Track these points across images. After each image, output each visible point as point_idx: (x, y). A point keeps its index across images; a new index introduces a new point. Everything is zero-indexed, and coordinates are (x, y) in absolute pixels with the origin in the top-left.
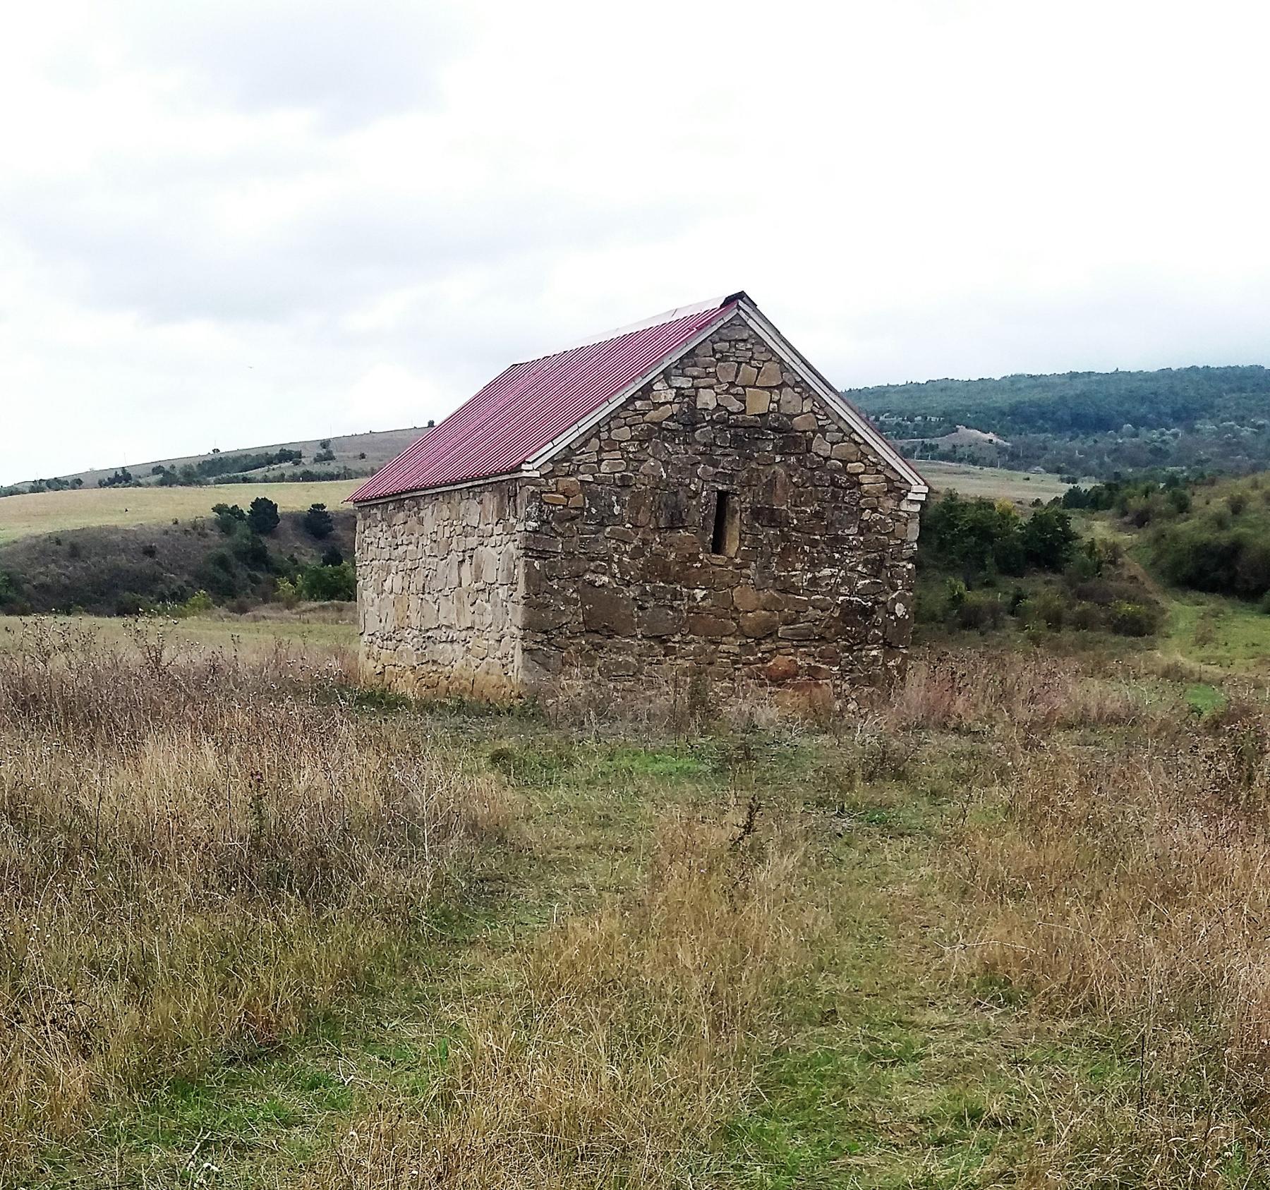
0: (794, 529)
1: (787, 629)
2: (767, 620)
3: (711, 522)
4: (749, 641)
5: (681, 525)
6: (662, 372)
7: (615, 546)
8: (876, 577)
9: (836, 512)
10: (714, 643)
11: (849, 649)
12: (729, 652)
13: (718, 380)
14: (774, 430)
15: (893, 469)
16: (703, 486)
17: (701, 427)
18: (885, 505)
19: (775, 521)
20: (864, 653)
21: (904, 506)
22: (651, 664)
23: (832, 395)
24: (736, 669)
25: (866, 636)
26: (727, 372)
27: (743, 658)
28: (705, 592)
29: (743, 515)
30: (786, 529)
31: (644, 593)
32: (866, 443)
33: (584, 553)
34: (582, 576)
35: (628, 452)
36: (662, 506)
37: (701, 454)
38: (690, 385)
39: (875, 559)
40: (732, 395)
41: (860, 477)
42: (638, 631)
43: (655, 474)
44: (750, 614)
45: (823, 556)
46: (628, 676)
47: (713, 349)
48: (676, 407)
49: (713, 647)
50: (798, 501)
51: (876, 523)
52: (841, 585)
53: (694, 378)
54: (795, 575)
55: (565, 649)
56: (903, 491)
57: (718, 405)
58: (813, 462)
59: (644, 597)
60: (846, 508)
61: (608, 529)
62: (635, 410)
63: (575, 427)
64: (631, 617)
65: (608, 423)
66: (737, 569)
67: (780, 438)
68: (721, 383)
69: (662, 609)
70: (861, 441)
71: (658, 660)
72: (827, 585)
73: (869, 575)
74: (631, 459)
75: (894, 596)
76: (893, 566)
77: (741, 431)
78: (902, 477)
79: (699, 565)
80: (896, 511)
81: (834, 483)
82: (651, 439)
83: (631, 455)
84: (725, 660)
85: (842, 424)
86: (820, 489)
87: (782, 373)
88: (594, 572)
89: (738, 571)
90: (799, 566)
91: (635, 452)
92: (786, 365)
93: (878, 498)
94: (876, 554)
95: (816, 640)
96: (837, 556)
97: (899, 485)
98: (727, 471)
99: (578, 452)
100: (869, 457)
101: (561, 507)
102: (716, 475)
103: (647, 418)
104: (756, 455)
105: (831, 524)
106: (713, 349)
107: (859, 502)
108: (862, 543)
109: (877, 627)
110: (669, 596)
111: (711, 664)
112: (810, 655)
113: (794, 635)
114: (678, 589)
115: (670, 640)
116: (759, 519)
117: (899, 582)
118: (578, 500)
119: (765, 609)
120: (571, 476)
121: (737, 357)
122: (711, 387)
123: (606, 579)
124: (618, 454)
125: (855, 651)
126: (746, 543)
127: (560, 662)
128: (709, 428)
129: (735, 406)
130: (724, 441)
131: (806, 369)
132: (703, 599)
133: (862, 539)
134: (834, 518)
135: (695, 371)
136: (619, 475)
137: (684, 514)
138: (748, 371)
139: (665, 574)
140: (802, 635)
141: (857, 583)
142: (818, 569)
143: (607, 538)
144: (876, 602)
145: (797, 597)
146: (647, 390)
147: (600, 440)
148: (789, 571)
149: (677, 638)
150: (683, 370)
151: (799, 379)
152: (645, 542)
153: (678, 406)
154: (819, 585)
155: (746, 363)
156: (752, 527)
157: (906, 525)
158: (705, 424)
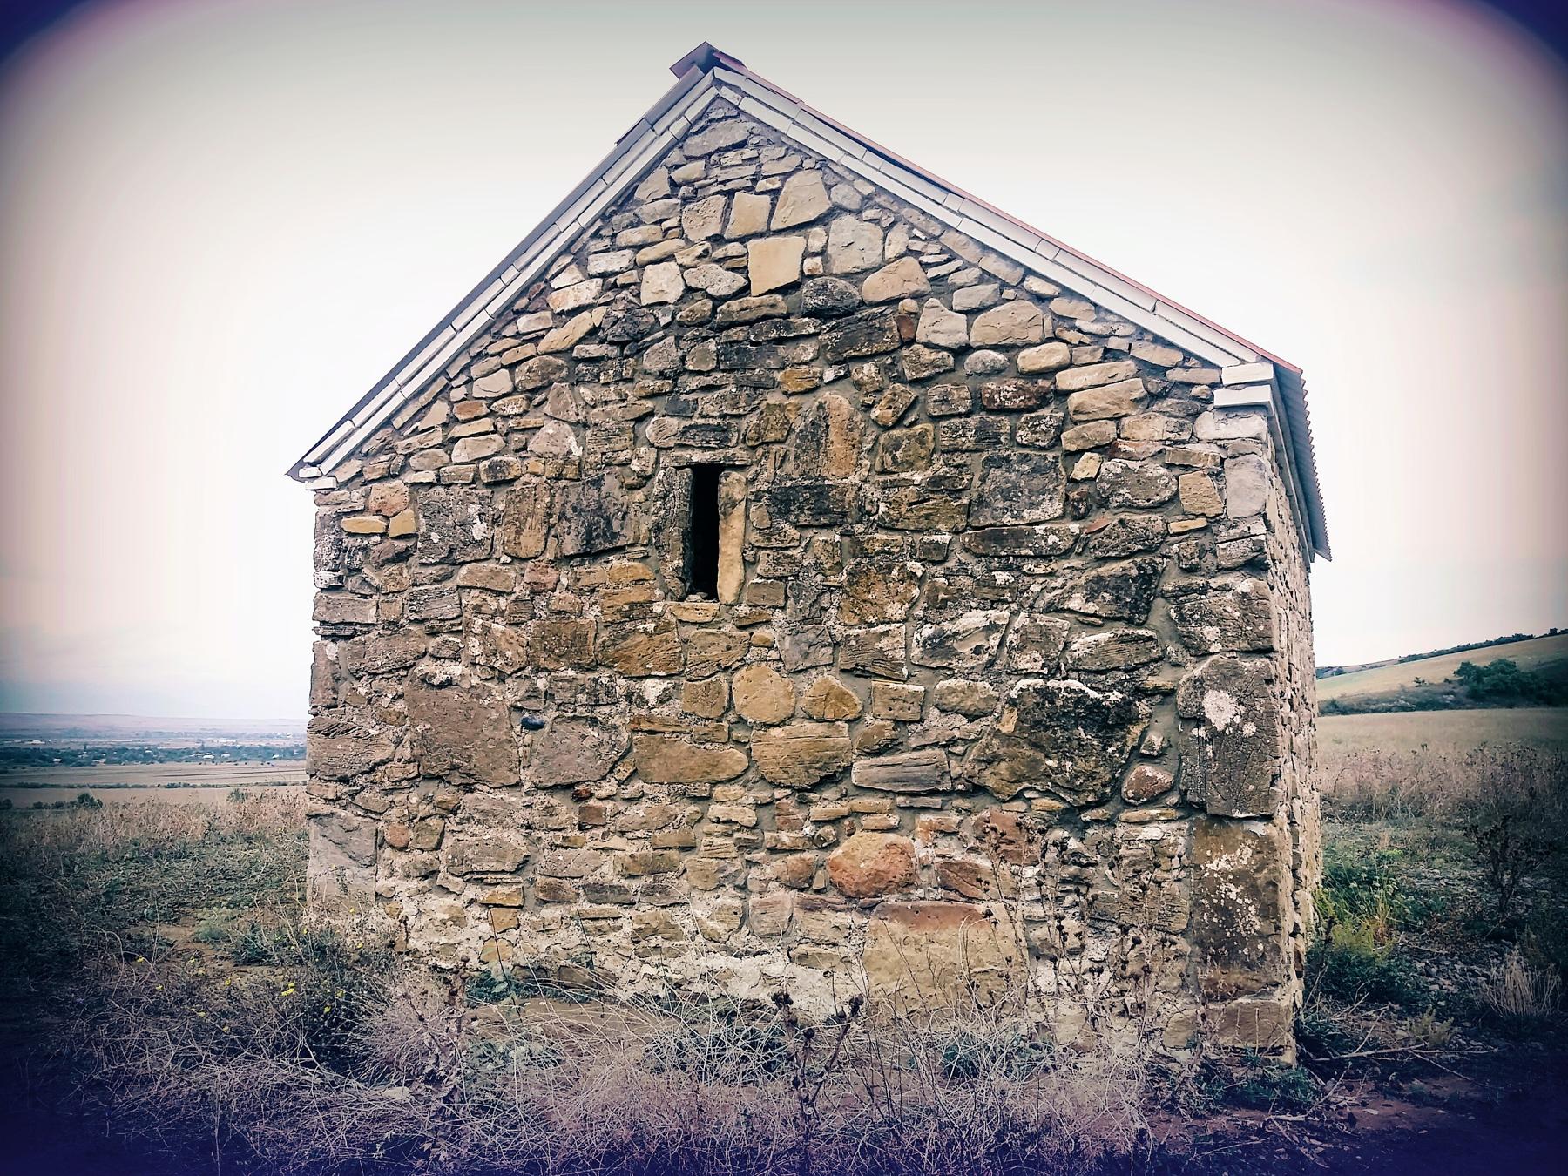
0: (881, 526)
1: (872, 766)
2: (816, 744)
3: (673, 534)
4: (778, 793)
5: (608, 546)
6: (565, 251)
7: (478, 601)
8: (1130, 622)
9: (995, 472)
10: (696, 799)
11: (1069, 817)
12: (729, 822)
13: (687, 240)
14: (811, 314)
15: (1158, 340)
16: (657, 461)
17: (653, 342)
18: (1140, 434)
19: (827, 512)
20: (1120, 831)
21: (1208, 425)
22: (553, 847)
23: (952, 202)
24: (751, 863)
25: (1116, 784)
26: (704, 220)
27: (767, 835)
28: (665, 684)
29: (753, 509)
30: (859, 528)
31: (533, 694)
32: (1067, 292)
33: (423, 621)
34: (411, 666)
35: (508, 416)
36: (569, 513)
37: (652, 396)
38: (625, 263)
39: (1124, 577)
40: (718, 261)
41: (1058, 375)
42: (524, 775)
43: (556, 450)
44: (775, 732)
45: (965, 582)
46: (503, 872)
47: (670, 178)
48: (597, 316)
49: (693, 808)
50: (889, 459)
51: (1117, 482)
52: (1021, 648)
53: (638, 248)
54: (886, 633)
55: (381, 814)
56: (1195, 391)
57: (689, 290)
58: (917, 364)
59: (533, 701)
60: (1025, 459)
61: (464, 570)
62: (517, 335)
63: (393, 386)
64: (507, 746)
65: (466, 368)
66: (742, 628)
67: (832, 329)
68: (693, 244)
69: (573, 724)
70: (1047, 289)
71: (565, 839)
72: (978, 650)
73: (1106, 619)
74: (512, 430)
75: (1197, 672)
76: (1186, 590)
77: (737, 333)
78: (1188, 355)
79: (651, 626)
80: (1175, 442)
81: (980, 404)
82: (551, 384)
83: (511, 423)
84: (717, 841)
85: (991, 264)
86: (944, 423)
87: (829, 188)
88: (436, 658)
89: (746, 633)
90: (895, 610)
91: (520, 415)
92: (836, 169)
93: (1117, 419)
94: (1125, 564)
95: (962, 794)
96: (1002, 577)
97: (1177, 375)
98: (711, 421)
99: (409, 431)
100: (1077, 324)
101: (378, 539)
102: (683, 433)
103: (543, 345)
104: (778, 376)
105: (981, 501)
106: (673, 183)
107: (1058, 439)
108: (1077, 539)
109: (1148, 758)
110: (583, 698)
111: (687, 848)
112: (946, 834)
113: (895, 780)
114: (604, 680)
115: (592, 795)
116: (789, 512)
117: (1211, 632)
118: (403, 523)
119: (811, 718)
120: (395, 477)
121: (723, 183)
122: (670, 257)
123: (455, 670)
124: (486, 425)
125: (1088, 825)
126: (759, 569)
127: (371, 842)
128: (671, 339)
129: (722, 282)
130: (703, 360)
131: (878, 162)
132: (664, 699)
133: (1075, 528)
134: (989, 486)
135: (635, 236)
136: (486, 463)
137: (616, 524)
138: (750, 209)
139: (575, 650)
140: (917, 780)
141: (1067, 645)
142: (948, 614)
143: (458, 587)
144: (1141, 692)
145: (892, 685)
146: (538, 290)
147: (451, 404)
148: (871, 625)
149: (608, 788)
150: (614, 235)
151: (868, 190)
152: (536, 590)
153: (603, 309)
154: (951, 653)
155: (748, 189)
156: (768, 533)
157: (1217, 475)
158: (660, 334)
